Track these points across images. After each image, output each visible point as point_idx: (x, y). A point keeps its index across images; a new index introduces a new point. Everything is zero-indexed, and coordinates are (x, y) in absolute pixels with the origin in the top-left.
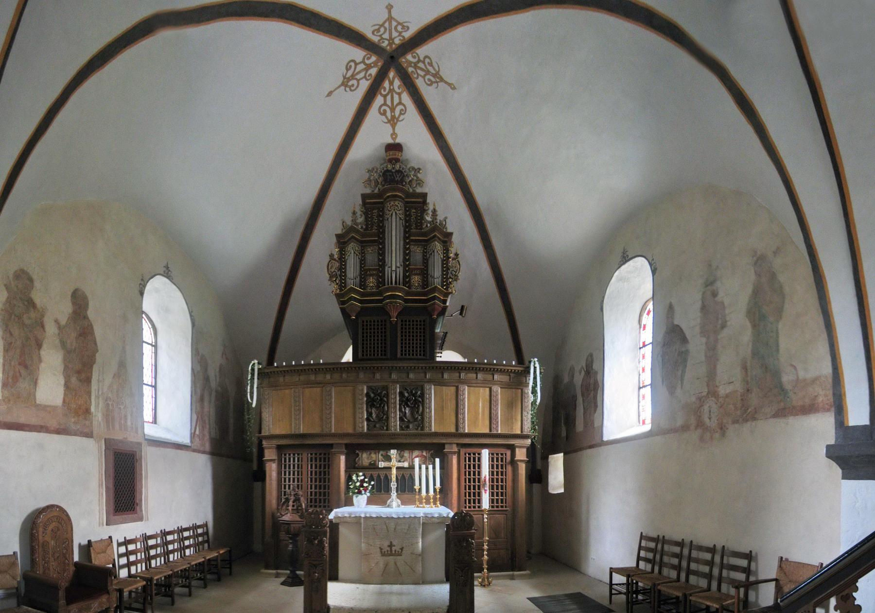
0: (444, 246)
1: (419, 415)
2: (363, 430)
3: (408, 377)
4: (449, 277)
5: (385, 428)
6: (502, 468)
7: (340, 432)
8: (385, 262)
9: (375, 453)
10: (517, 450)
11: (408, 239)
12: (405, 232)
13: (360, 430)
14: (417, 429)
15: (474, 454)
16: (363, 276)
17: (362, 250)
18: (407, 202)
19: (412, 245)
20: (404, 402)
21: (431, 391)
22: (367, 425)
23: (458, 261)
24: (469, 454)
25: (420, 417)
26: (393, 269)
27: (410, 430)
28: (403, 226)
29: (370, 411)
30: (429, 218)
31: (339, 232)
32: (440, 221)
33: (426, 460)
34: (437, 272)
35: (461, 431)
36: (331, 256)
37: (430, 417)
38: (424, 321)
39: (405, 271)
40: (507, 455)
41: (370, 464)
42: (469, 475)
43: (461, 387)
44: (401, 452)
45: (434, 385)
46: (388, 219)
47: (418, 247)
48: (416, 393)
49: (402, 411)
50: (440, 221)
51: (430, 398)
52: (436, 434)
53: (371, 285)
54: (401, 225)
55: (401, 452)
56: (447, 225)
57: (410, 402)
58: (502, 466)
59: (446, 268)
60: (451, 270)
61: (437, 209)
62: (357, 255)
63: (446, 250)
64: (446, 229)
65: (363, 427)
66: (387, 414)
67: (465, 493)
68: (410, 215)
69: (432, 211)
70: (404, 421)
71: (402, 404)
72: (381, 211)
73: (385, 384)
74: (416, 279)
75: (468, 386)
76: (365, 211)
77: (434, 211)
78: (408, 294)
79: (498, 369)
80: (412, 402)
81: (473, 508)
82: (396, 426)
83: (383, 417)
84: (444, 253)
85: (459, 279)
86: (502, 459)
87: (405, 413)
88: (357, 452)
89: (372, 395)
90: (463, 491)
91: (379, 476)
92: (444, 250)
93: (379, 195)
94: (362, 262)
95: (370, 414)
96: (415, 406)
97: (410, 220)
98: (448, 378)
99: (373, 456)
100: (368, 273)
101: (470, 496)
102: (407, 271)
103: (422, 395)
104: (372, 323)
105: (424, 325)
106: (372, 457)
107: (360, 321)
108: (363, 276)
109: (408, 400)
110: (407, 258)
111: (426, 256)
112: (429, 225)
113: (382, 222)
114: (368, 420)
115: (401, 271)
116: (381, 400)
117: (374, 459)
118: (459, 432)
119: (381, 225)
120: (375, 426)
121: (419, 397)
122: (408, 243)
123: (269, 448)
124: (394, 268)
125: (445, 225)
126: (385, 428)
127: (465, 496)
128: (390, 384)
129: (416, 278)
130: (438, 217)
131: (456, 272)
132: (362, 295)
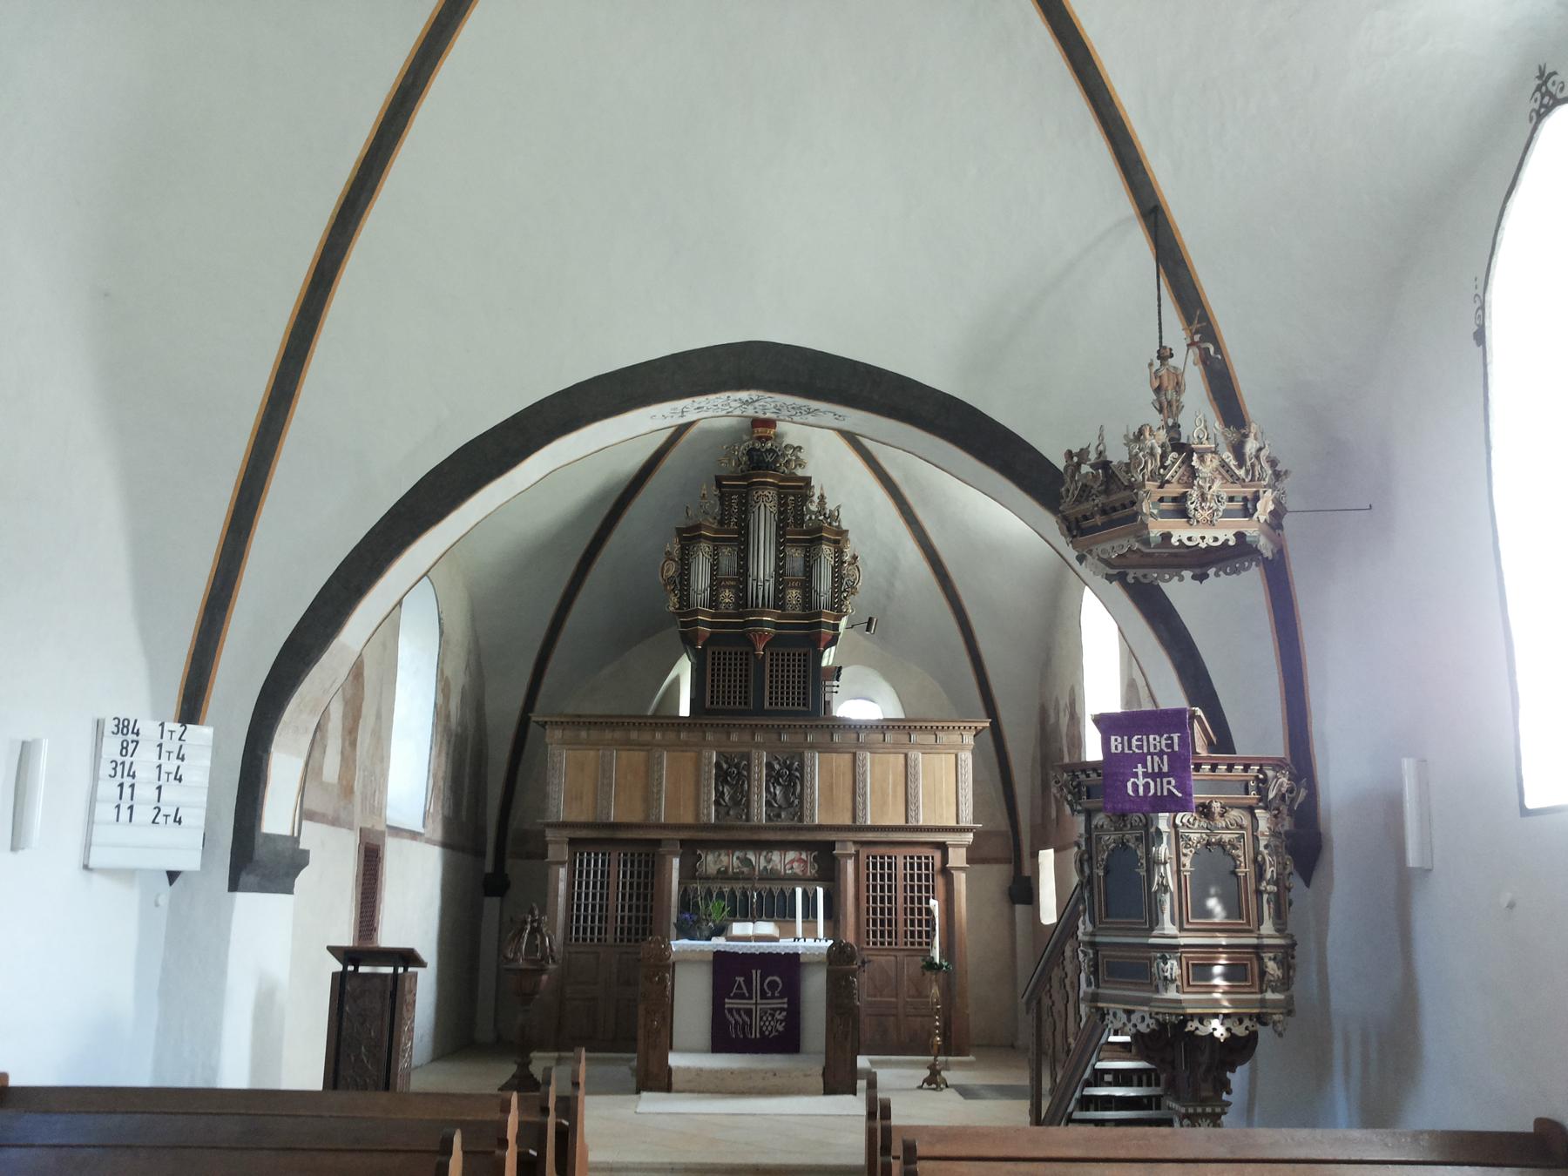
2: (710, 819)
5: (744, 817)
7: (672, 821)
8: (748, 570)
9: (729, 856)
10: (950, 850)
11: (781, 543)
13: (704, 819)
14: (793, 820)
15: (882, 857)
17: (714, 550)
19: (789, 546)
20: (774, 777)
21: (814, 761)
24: (875, 857)
25: (796, 802)
26: (759, 584)
27: (782, 821)
28: (775, 520)
29: (721, 788)
30: (814, 508)
33: (807, 867)
34: (824, 584)
35: (860, 822)
37: (812, 802)
38: (805, 655)
39: (777, 583)
41: (719, 871)
43: (861, 755)
45: (819, 752)
48: (792, 764)
49: (770, 792)
51: (813, 771)
52: (820, 828)
53: (727, 600)
55: (768, 853)
58: (927, 876)
63: (839, 553)
65: (709, 814)
66: (748, 794)
68: (786, 504)
70: (773, 806)
72: (743, 498)
73: (745, 750)
74: (793, 595)
75: (871, 753)
77: (822, 497)
83: (742, 799)
84: (835, 557)
85: (858, 593)
87: (775, 794)
88: (699, 852)
89: (725, 766)
90: (864, 917)
91: (732, 892)
92: (836, 553)
94: (715, 567)
95: (720, 795)
99: (724, 859)
100: (723, 583)
102: (780, 584)
103: (801, 768)
107: (709, 653)
109: (779, 775)
111: (809, 562)
112: (813, 517)
113: (746, 512)
114: (717, 803)
116: (739, 773)
117: (725, 863)
118: (858, 823)
120: (728, 813)
121: (796, 770)
123: (556, 842)
125: (838, 517)
126: (744, 817)
127: (868, 925)
129: (794, 592)
132: (713, 616)
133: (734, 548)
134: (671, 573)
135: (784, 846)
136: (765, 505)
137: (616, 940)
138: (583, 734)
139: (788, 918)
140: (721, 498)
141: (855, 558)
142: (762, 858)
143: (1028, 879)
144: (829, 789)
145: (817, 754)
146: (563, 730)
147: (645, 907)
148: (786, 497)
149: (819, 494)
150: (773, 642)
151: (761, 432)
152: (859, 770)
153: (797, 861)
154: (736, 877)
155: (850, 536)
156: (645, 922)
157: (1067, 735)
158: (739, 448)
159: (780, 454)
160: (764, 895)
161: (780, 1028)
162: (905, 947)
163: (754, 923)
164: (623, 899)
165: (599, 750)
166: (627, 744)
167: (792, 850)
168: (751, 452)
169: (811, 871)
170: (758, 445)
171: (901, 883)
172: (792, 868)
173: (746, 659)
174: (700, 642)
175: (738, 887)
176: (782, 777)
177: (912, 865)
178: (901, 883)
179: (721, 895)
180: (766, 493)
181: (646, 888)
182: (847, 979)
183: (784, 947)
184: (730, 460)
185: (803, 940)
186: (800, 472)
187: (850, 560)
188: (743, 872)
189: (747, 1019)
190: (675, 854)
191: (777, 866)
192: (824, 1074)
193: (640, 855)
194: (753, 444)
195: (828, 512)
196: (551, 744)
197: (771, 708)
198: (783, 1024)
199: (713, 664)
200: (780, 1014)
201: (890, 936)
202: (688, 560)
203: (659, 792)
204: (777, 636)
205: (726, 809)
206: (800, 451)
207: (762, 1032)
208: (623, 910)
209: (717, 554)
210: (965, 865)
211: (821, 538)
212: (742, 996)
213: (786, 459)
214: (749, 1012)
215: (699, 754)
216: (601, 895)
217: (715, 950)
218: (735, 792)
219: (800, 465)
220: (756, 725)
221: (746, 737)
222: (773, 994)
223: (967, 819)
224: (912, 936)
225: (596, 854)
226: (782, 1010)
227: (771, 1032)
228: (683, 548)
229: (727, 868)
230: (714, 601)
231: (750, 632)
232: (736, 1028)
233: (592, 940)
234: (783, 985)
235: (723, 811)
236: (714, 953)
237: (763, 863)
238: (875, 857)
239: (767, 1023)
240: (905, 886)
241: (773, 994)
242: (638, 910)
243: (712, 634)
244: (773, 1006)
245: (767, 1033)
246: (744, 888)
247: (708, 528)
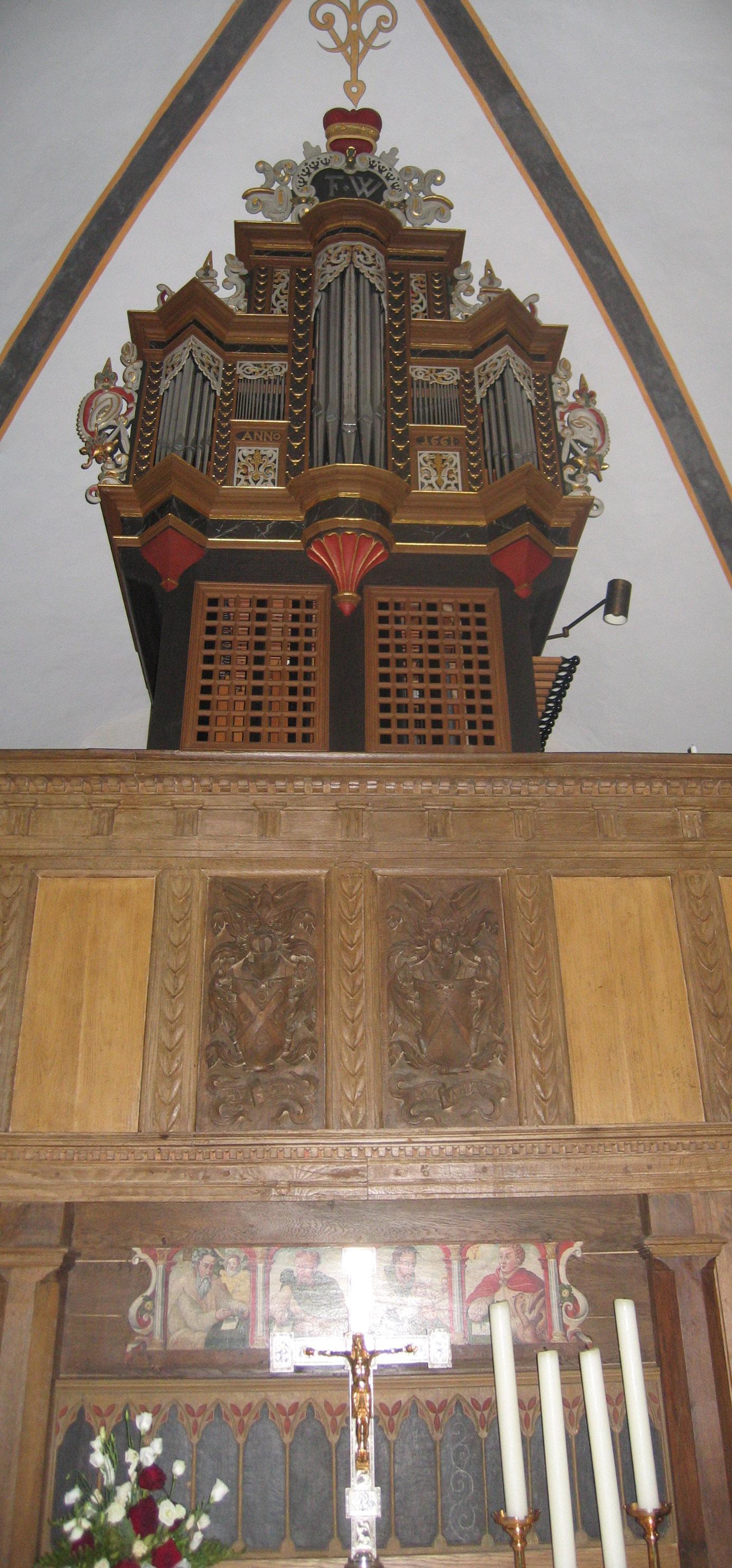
148: (405, 273)
159: (389, 184)
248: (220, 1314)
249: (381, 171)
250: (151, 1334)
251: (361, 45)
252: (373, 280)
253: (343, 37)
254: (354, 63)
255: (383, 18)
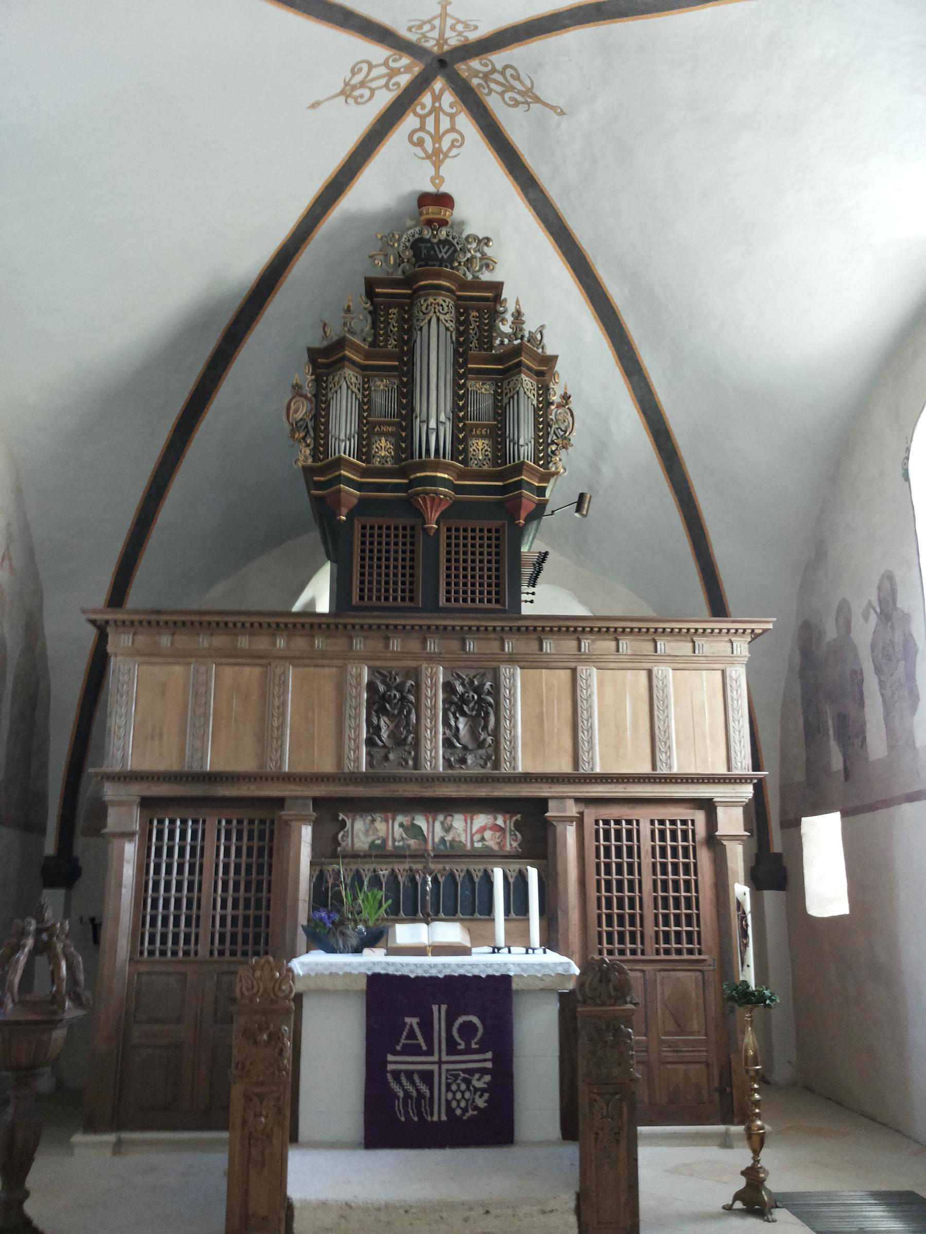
0: (538, 382)
1: (489, 735)
3: (463, 648)
4: (549, 441)
5: (411, 763)
6: (686, 855)
7: (300, 770)
9: (387, 821)
10: (720, 811)
12: (456, 353)
13: (350, 767)
14: (484, 767)
15: (618, 822)
16: (365, 435)
17: (364, 383)
18: (460, 298)
22: (369, 754)
23: (569, 409)
24: (606, 822)
25: (489, 739)
27: (468, 768)
28: (452, 342)
29: (375, 721)
30: (506, 328)
31: (318, 344)
32: (530, 332)
33: (505, 837)
35: (585, 769)
36: (297, 389)
37: (513, 740)
38: (497, 531)
39: (455, 430)
40: (696, 823)
41: (372, 845)
42: (608, 872)
43: (583, 670)
44: (445, 818)
46: (421, 329)
47: (483, 384)
48: (482, 685)
50: (530, 332)
51: (513, 696)
52: (527, 778)
53: (383, 453)
54: (449, 341)
55: (445, 818)
56: (545, 341)
57: (467, 705)
58: (685, 849)
59: (543, 424)
60: (554, 427)
61: (523, 310)
62: (352, 392)
63: (544, 390)
64: (543, 348)
65: (358, 759)
66: (417, 731)
67: (599, 916)
68: (466, 322)
69: (513, 315)
70: (455, 747)
71: (449, 709)
72: (407, 312)
73: (413, 664)
74: (480, 447)
76: (371, 308)
77: (518, 315)
78: (461, 475)
79: (664, 629)
80: (471, 706)
81: (631, 954)
82: (436, 758)
83: (406, 738)
84: (539, 395)
86: (685, 833)
87: (457, 729)
88: (341, 816)
89: (382, 688)
90: (593, 912)
91: (393, 875)
92: (539, 389)
93: (407, 281)
94: (365, 406)
95: (374, 730)
96: (478, 715)
97: (466, 331)
98: (553, 652)
99: (381, 826)
100: (377, 429)
101: (610, 924)
102: (461, 430)
103: (496, 690)
104: (384, 532)
105: (497, 554)
106: (376, 829)
108: (365, 435)
109: (463, 700)
110: (461, 403)
111: (501, 401)
112: (506, 341)
113: (409, 331)
114: (370, 742)
115: (447, 431)
116: (403, 698)
118: (582, 771)
119: (406, 337)
120: (386, 758)
121: (489, 693)
122: (461, 376)
123: (121, 803)
124: (433, 424)
126: (411, 763)
127: (600, 925)
128: (424, 665)
130: (524, 326)
131: (566, 432)
132: (364, 473)
133: (392, 380)
134: (299, 415)
135: (471, 805)
136: (438, 319)
137: (212, 953)
138: (165, 641)
139: (477, 916)
140: (373, 313)
141: (566, 398)
142: (438, 825)
143: (779, 856)
144: (537, 720)
145: (519, 671)
146: (134, 634)
147: (259, 902)
148: (467, 312)
149: (514, 310)
150: (453, 511)
151: (433, 213)
152: (582, 694)
153: (491, 829)
154: (399, 855)
155: (559, 367)
156: (257, 923)
157: (873, 647)
158: (400, 237)
159: (458, 247)
160: (441, 880)
161: (481, 1103)
162: (658, 957)
163: (428, 924)
164: (225, 889)
165: (189, 664)
166: (233, 656)
167: (481, 812)
168: (417, 245)
169: (511, 844)
170: (427, 234)
171: (647, 860)
172: (483, 839)
173: (412, 536)
174: (344, 510)
175: (401, 868)
176: (467, 703)
177: (662, 833)
178: (647, 860)
179: (376, 881)
180: (440, 300)
181: (260, 871)
182: (617, 1030)
183: (486, 965)
184: (386, 255)
185: (506, 950)
186: (486, 276)
187: (559, 400)
188: (409, 846)
189: (424, 1089)
190: (304, 820)
191: (459, 836)
192: (578, 1211)
193: (251, 822)
194: (421, 233)
195: (527, 335)
196: (116, 656)
197: (448, 605)
198: (486, 1096)
199: (363, 543)
200: (479, 1080)
201: (633, 941)
202: (326, 395)
203: (282, 726)
204: (456, 503)
205: (383, 752)
206: (487, 244)
207: (450, 1111)
208: (224, 906)
209: (369, 388)
210: (742, 832)
211: (519, 364)
212: (416, 1050)
213: (469, 255)
214: (427, 1077)
215: (343, 669)
216: (191, 884)
217: (369, 973)
218: (397, 727)
219: (487, 266)
220: (429, 627)
221: (414, 645)
222: (468, 1044)
223: (743, 763)
224: (667, 941)
225: (184, 822)
226: (483, 1071)
227: (465, 1110)
228: (318, 381)
229: (385, 841)
230: (364, 451)
231: (417, 494)
232: (405, 1105)
233: (175, 953)
234: (485, 1028)
235: (378, 753)
236: (368, 976)
237: (439, 832)
238: (606, 822)
239: (459, 1096)
240: (654, 864)
241: (468, 1044)
242: (247, 906)
243: (361, 500)
244: (470, 1066)
245: (458, 1112)
246: (411, 870)
247: (356, 348)
248: (374, 837)
249: (453, 238)
250: (347, 845)
251: (441, 156)
252: (447, 325)
253: (430, 150)
254: (437, 166)
255: (457, 140)
